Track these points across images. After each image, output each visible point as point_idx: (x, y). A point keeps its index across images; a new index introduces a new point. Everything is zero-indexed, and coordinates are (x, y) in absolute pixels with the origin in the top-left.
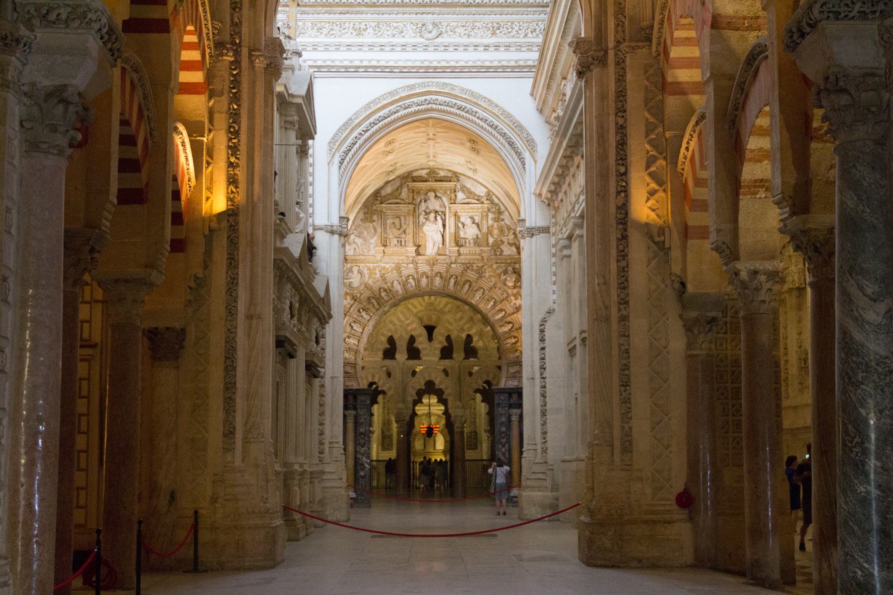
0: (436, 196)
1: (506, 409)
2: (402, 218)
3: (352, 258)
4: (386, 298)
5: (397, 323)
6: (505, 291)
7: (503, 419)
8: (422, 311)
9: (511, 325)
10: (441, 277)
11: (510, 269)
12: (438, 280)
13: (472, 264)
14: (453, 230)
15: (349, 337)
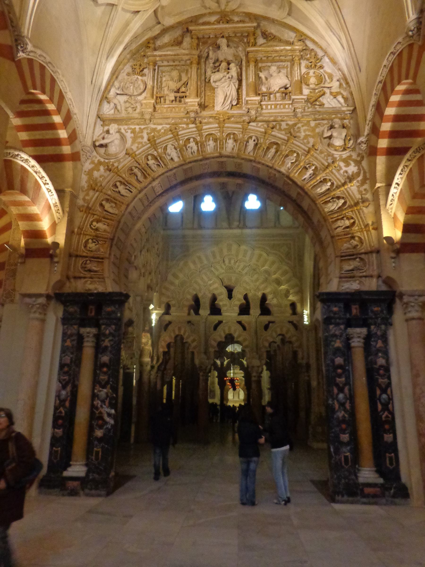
0: (228, 46)
1: (342, 327)
2: (183, 75)
3: (112, 117)
4: (154, 167)
6: (329, 155)
8: (223, 273)
9: (342, 201)
10: (235, 141)
11: (337, 122)
12: (230, 143)
14: (252, 78)
15: (98, 221)
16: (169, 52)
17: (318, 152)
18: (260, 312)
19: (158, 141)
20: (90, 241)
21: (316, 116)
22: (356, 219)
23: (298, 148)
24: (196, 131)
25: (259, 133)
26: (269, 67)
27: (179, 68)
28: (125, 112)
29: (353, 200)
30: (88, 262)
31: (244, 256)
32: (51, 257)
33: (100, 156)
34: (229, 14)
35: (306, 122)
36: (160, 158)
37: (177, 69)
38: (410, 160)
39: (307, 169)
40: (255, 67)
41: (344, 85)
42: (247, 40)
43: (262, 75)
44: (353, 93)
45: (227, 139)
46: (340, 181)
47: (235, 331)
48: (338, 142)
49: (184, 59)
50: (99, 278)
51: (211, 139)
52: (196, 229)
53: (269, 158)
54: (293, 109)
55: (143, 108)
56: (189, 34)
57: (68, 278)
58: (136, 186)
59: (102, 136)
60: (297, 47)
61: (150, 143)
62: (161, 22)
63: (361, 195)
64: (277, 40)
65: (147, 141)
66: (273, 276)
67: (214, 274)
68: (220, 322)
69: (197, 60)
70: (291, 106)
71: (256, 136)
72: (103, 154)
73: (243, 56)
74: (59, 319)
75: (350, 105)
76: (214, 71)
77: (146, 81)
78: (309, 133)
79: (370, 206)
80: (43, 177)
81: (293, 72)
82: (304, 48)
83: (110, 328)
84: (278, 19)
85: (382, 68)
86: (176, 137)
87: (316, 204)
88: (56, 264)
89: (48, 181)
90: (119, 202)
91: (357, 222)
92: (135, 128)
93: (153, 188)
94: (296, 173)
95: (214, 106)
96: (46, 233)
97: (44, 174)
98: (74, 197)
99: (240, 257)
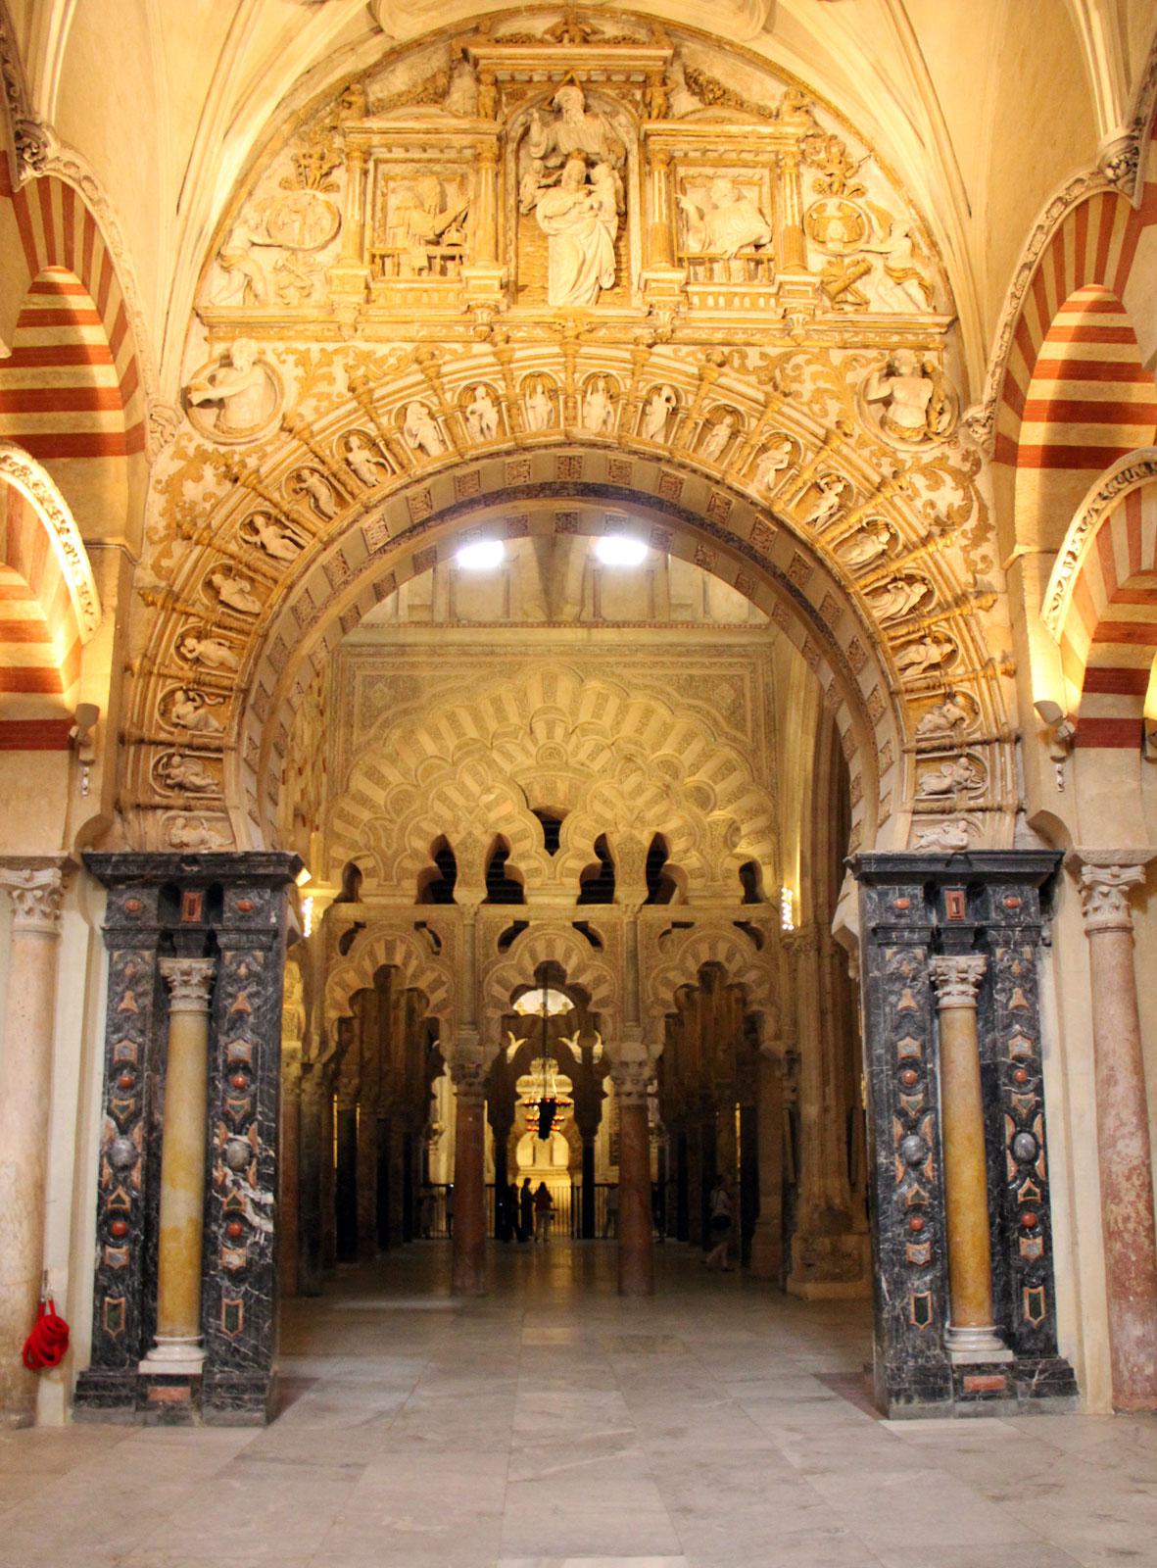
0: (586, 109)
1: (919, 952)
2: (452, 190)
3: (237, 315)
4: (369, 472)
5: (460, 800)
6: (884, 452)
7: (907, 1000)
8: (529, 769)
9: (920, 589)
13: (740, 348)
14: (658, 213)
15: (201, 635)
16: (410, 121)
17: (851, 441)
18: (645, 894)
19: (377, 395)
20: (180, 695)
21: (847, 336)
22: (958, 642)
23: (794, 427)
24: (493, 365)
25: (682, 378)
26: (711, 178)
27: (437, 168)
28: (279, 300)
29: (951, 589)
30: (176, 760)
31: (597, 714)
32: (73, 746)
33: (203, 436)
34: (590, 13)
35: (816, 350)
36: (387, 445)
37: (433, 173)
38: (1105, 498)
39: (822, 491)
40: (668, 177)
41: (925, 250)
42: (644, 95)
43: (688, 203)
44: (950, 275)
45: (585, 392)
46: (915, 531)
47: (568, 955)
48: (908, 416)
49: (457, 145)
50: (208, 809)
51: (539, 389)
52: (441, 625)
53: (710, 454)
54: (781, 312)
55: (334, 293)
56: (468, 68)
57: (119, 808)
58: (313, 529)
59: (207, 373)
60: (790, 130)
61: (357, 398)
62: (384, 27)
63: (974, 573)
64: (732, 103)
65: (345, 390)
66: (688, 780)
67: (501, 771)
68: (520, 926)
69: (495, 150)
70: (773, 301)
71: (672, 387)
72: (212, 430)
73: (631, 140)
74: (99, 932)
75: (941, 309)
76: (544, 182)
77: (341, 206)
78: (827, 386)
79: (997, 605)
80: (59, 512)
81: (779, 200)
82: (810, 133)
83: (249, 959)
84: (736, 40)
85: (1032, 232)
86: (433, 379)
87: (847, 596)
88: (87, 769)
89: (72, 524)
90: (265, 575)
91: (961, 651)
92: (308, 350)
93: (363, 533)
94: (790, 500)
95: (544, 288)
96: (58, 677)
97: (60, 503)
98: (129, 561)
99: (585, 716)
